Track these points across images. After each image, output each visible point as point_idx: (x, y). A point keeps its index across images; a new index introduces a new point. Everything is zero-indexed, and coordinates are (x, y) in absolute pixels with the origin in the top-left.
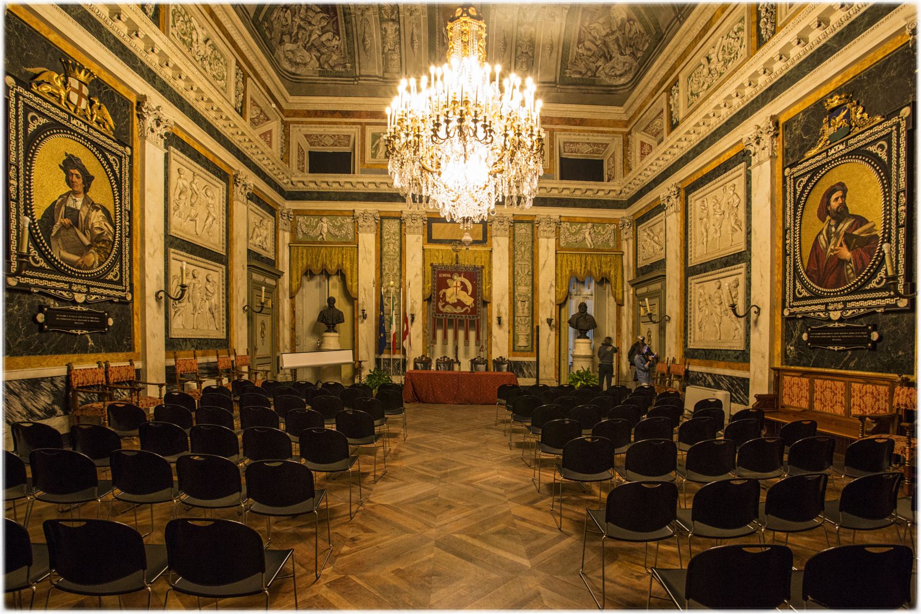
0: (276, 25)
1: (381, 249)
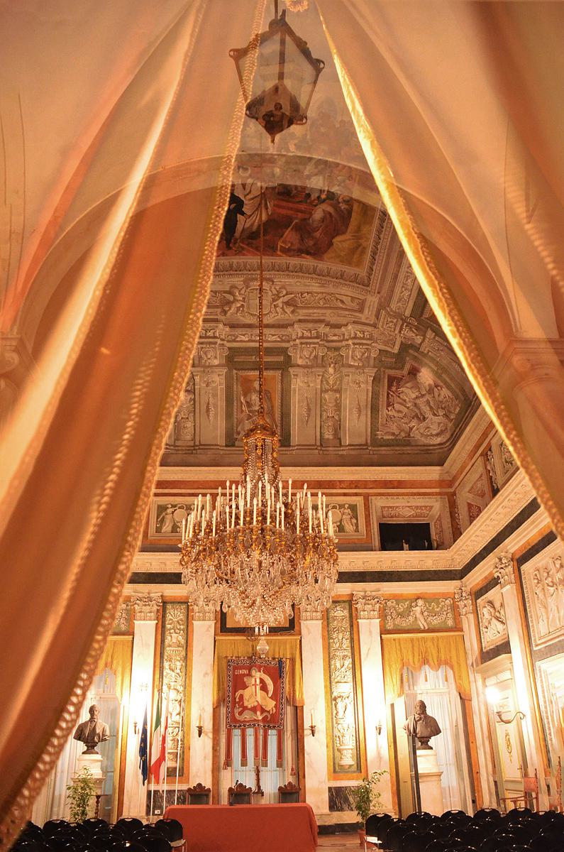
1: (163, 641)
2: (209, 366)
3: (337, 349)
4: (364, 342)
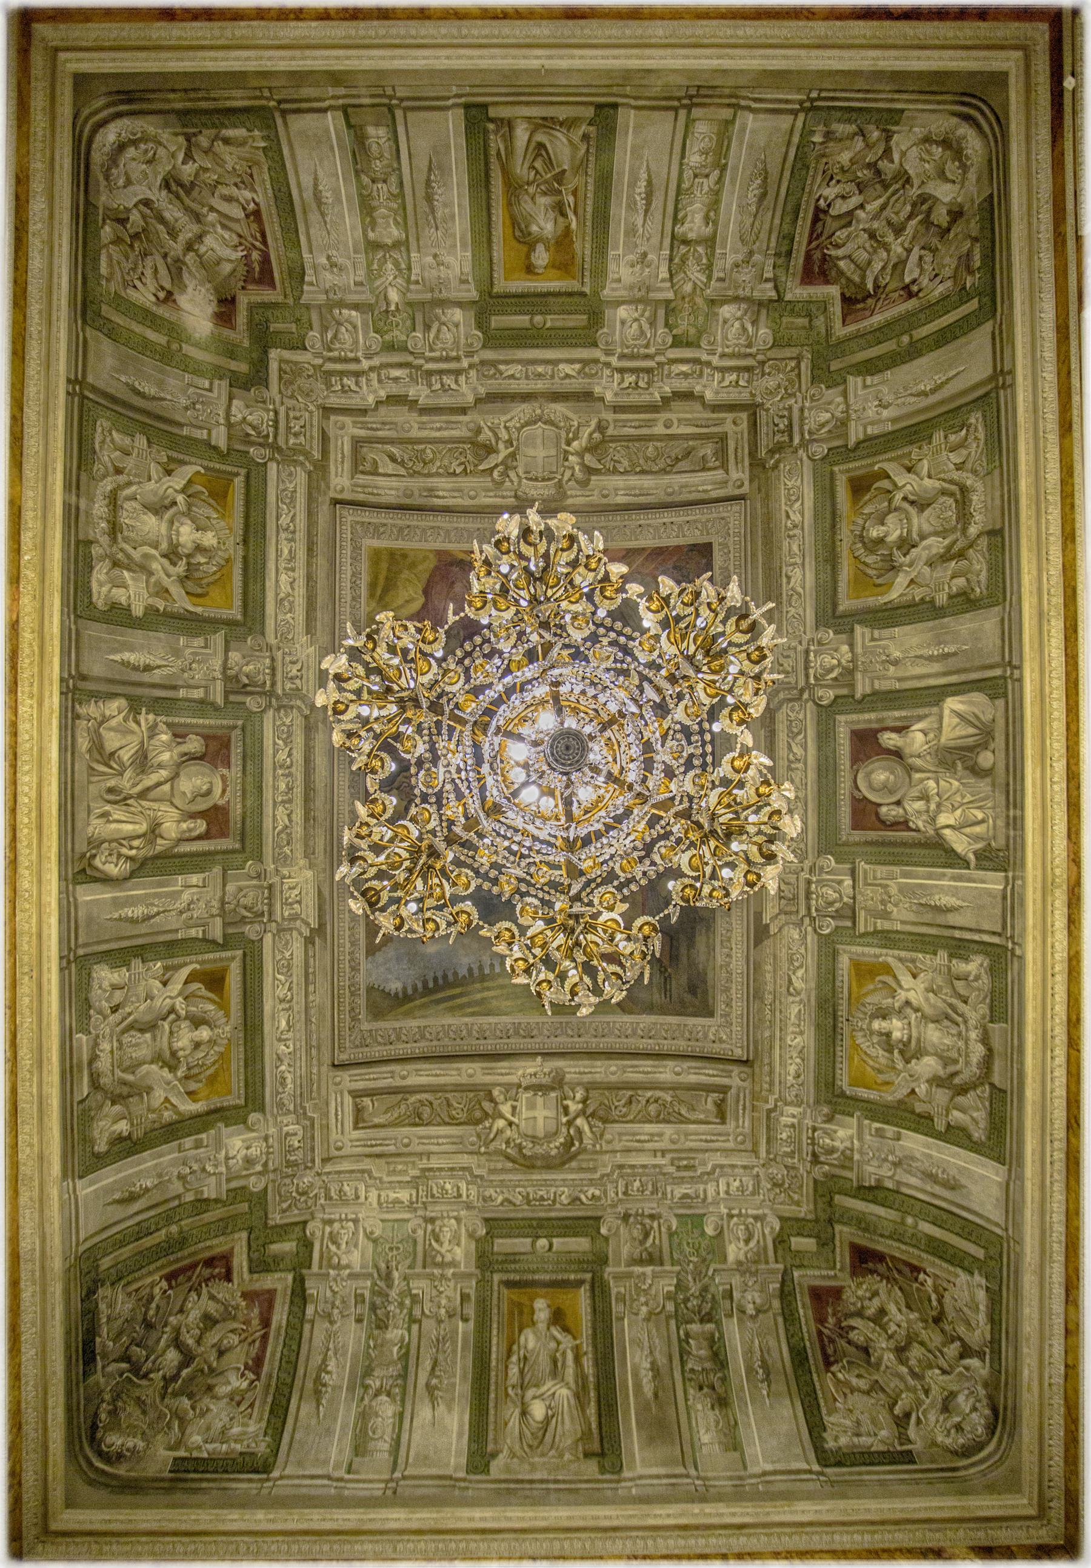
0: (949, 263)
2: (639, 301)
3: (390, 347)
4: (338, 367)
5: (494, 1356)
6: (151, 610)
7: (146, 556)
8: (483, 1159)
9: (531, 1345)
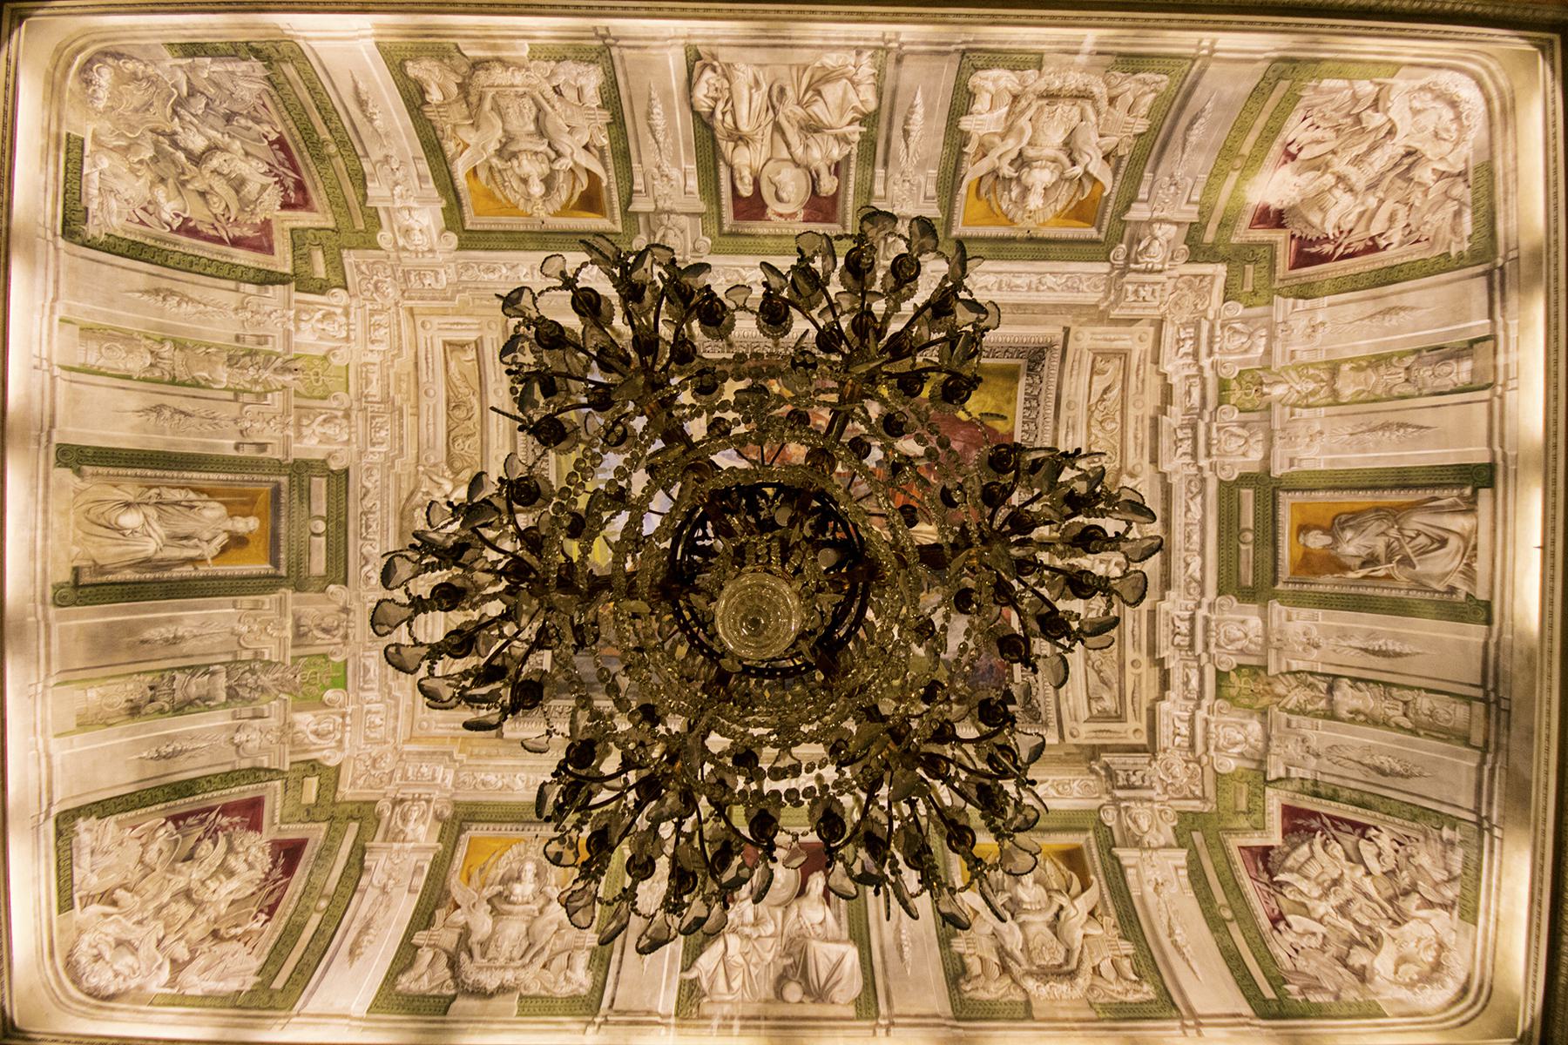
2: (1267, 639)
3: (1223, 386)
5: (195, 475)
6: (965, 138)
7: (1022, 132)
8: (412, 469)
9: (207, 513)
